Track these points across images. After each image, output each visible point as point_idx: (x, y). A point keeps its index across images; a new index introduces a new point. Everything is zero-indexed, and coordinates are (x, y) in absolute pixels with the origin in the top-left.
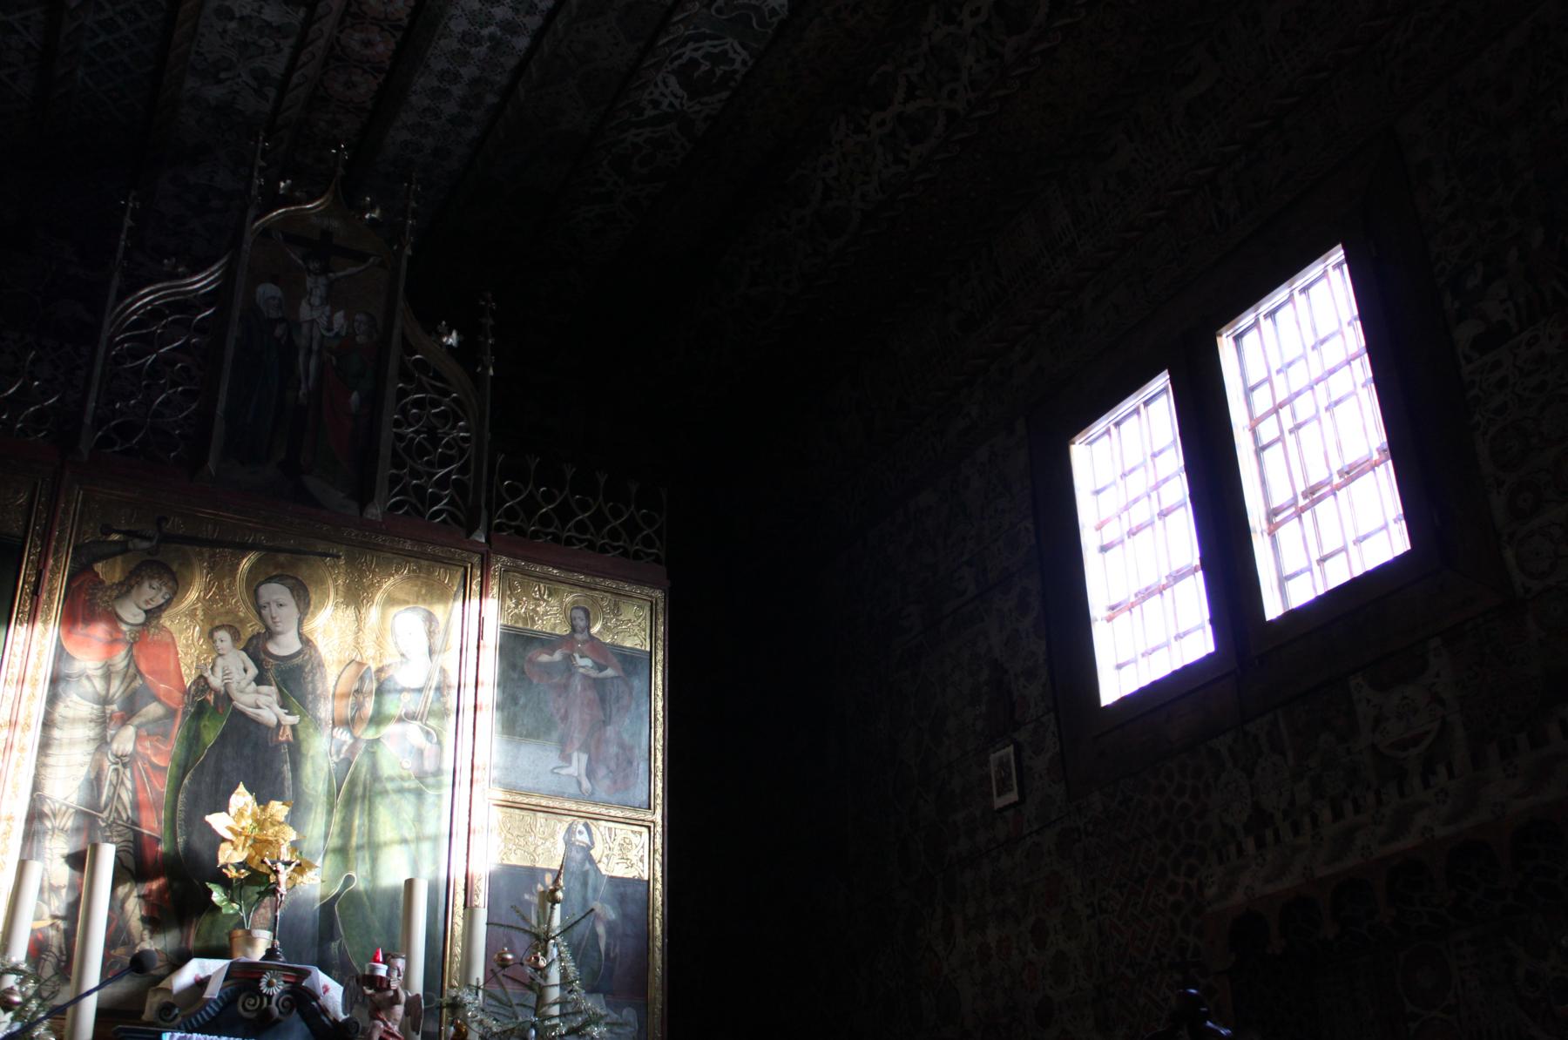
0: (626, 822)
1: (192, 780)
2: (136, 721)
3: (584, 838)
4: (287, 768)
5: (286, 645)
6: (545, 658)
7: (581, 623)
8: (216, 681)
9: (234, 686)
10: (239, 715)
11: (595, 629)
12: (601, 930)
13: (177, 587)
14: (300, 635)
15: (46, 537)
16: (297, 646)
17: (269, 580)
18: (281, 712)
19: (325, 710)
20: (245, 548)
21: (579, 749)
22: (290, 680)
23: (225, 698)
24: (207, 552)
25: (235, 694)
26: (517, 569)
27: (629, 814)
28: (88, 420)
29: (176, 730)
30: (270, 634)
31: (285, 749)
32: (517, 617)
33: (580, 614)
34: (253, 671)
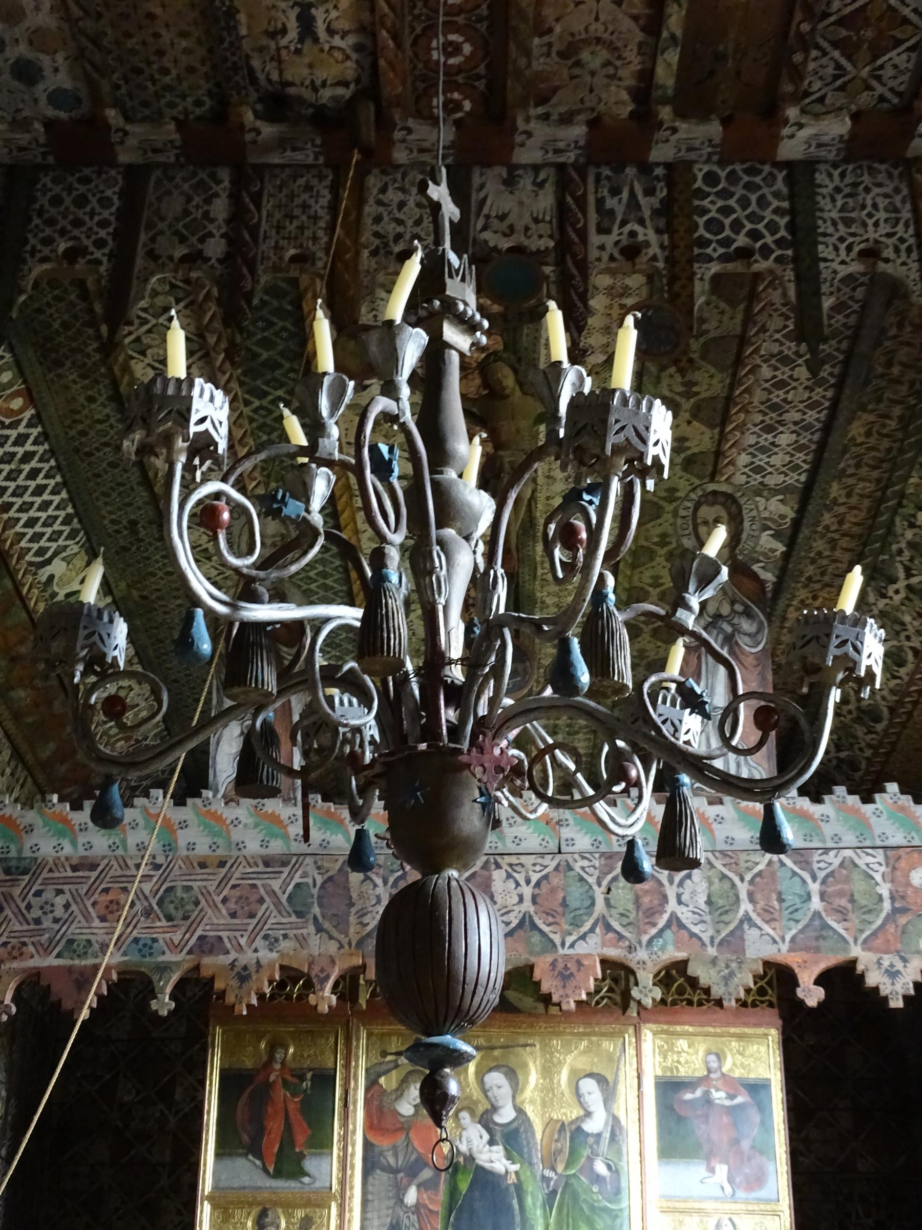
0: (763, 1213)
1: (456, 1219)
2: (416, 1181)
4: (515, 1202)
5: (506, 1115)
6: (688, 1096)
7: (714, 1065)
8: (463, 1148)
9: (475, 1149)
10: (480, 1169)
11: (724, 1070)
14: (515, 1106)
15: (347, 1066)
17: (490, 1070)
18: (507, 1163)
19: (537, 1157)
21: (721, 1162)
22: (512, 1138)
23: (470, 1158)
25: (476, 1155)
26: (663, 1032)
27: (762, 1207)
29: (443, 1187)
30: (495, 1109)
31: (512, 1189)
32: (665, 1069)
33: (713, 1058)
34: (486, 1137)
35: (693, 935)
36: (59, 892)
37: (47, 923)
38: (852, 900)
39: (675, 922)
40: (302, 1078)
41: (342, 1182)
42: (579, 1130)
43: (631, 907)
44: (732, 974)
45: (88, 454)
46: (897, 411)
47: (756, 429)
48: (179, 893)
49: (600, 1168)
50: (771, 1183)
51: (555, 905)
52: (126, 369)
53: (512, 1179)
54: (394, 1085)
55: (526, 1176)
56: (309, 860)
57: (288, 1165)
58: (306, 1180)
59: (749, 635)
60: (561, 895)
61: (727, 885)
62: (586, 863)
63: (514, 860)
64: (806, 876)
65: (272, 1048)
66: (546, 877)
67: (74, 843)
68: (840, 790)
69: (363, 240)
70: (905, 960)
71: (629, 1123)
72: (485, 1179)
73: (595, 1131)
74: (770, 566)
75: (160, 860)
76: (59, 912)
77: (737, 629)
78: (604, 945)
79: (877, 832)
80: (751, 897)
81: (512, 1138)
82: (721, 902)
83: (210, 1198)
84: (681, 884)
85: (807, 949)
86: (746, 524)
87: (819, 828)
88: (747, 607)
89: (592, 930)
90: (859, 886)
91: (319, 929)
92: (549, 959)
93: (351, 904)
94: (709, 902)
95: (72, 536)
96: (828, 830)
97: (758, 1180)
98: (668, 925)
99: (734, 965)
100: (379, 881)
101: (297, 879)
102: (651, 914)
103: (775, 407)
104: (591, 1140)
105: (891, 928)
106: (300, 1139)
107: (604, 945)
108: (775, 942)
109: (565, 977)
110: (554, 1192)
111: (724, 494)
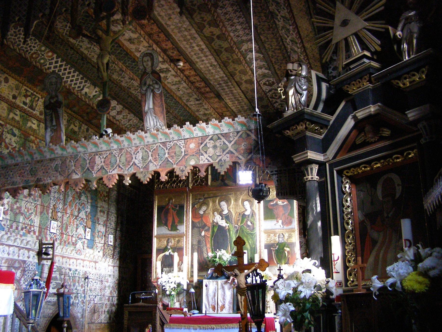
3: (282, 236)
5: (226, 212)
6: (272, 203)
8: (215, 221)
10: (219, 225)
12: (286, 252)
13: (208, 205)
15: (187, 203)
16: (227, 212)
20: (217, 196)
24: (211, 199)
25: (218, 222)
28: (190, 182)
30: (223, 211)
31: (227, 230)
34: (221, 218)
35: (138, 166)
36: (11, 171)
37: (9, 179)
38: (175, 154)
39: (134, 164)
40: (176, 207)
41: (186, 231)
42: (244, 214)
43: (125, 161)
44: (146, 175)
45: (76, 62)
46: (263, 15)
47: (229, 26)
48: (34, 169)
49: (249, 223)
50: (293, 224)
51: (108, 162)
52: (69, 41)
53: (227, 228)
54: (199, 207)
55: (231, 226)
56: (59, 158)
57: (174, 228)
58: (178, 231)
59: (157, 89)
60: (110, 160)
61: (147, 153)
62: (116, 152)
63: (100, 153)
64: (165, 149)
65: (169, 200)
66: (107, 156)
67: (15, 160)
68: (175, 126)
69: (79, 2)
70: (186, 167)
71: (256, 211)
72: (221, 228)
73: (248, 214)
74: (262, 60)
75: (30, 162)
76: (11, 176)
77: (154, 88)
78: (118, 171)
79: (183, 135)
80: (152, 156)
81: (227, 218)
82: (145, 158)
83: (156, 237)
84: (136, 154)
85: (163, 167)
86: (155, 60)
87: (169, 136)
88: (156, 81)
89: (116, 168)
90: (177, 149)
91: (60, 174)
92: (106, 176)
93: (67, 167)
94: (142, 158)
95: (86, 82)
96: (171, 136)
97: (290, 223)
98: (132, 165)
99: (146, 173)
100: (72, 161)
101: (56, 163)
102: (129, 162)
103: (229, 20)
104: (247, 216)
105: (183, 159)
106: (176, 221)
107: (118, 171)
108: (156, 166)
109: (109, 180)
110: (238, 230)
111: (149, 53)
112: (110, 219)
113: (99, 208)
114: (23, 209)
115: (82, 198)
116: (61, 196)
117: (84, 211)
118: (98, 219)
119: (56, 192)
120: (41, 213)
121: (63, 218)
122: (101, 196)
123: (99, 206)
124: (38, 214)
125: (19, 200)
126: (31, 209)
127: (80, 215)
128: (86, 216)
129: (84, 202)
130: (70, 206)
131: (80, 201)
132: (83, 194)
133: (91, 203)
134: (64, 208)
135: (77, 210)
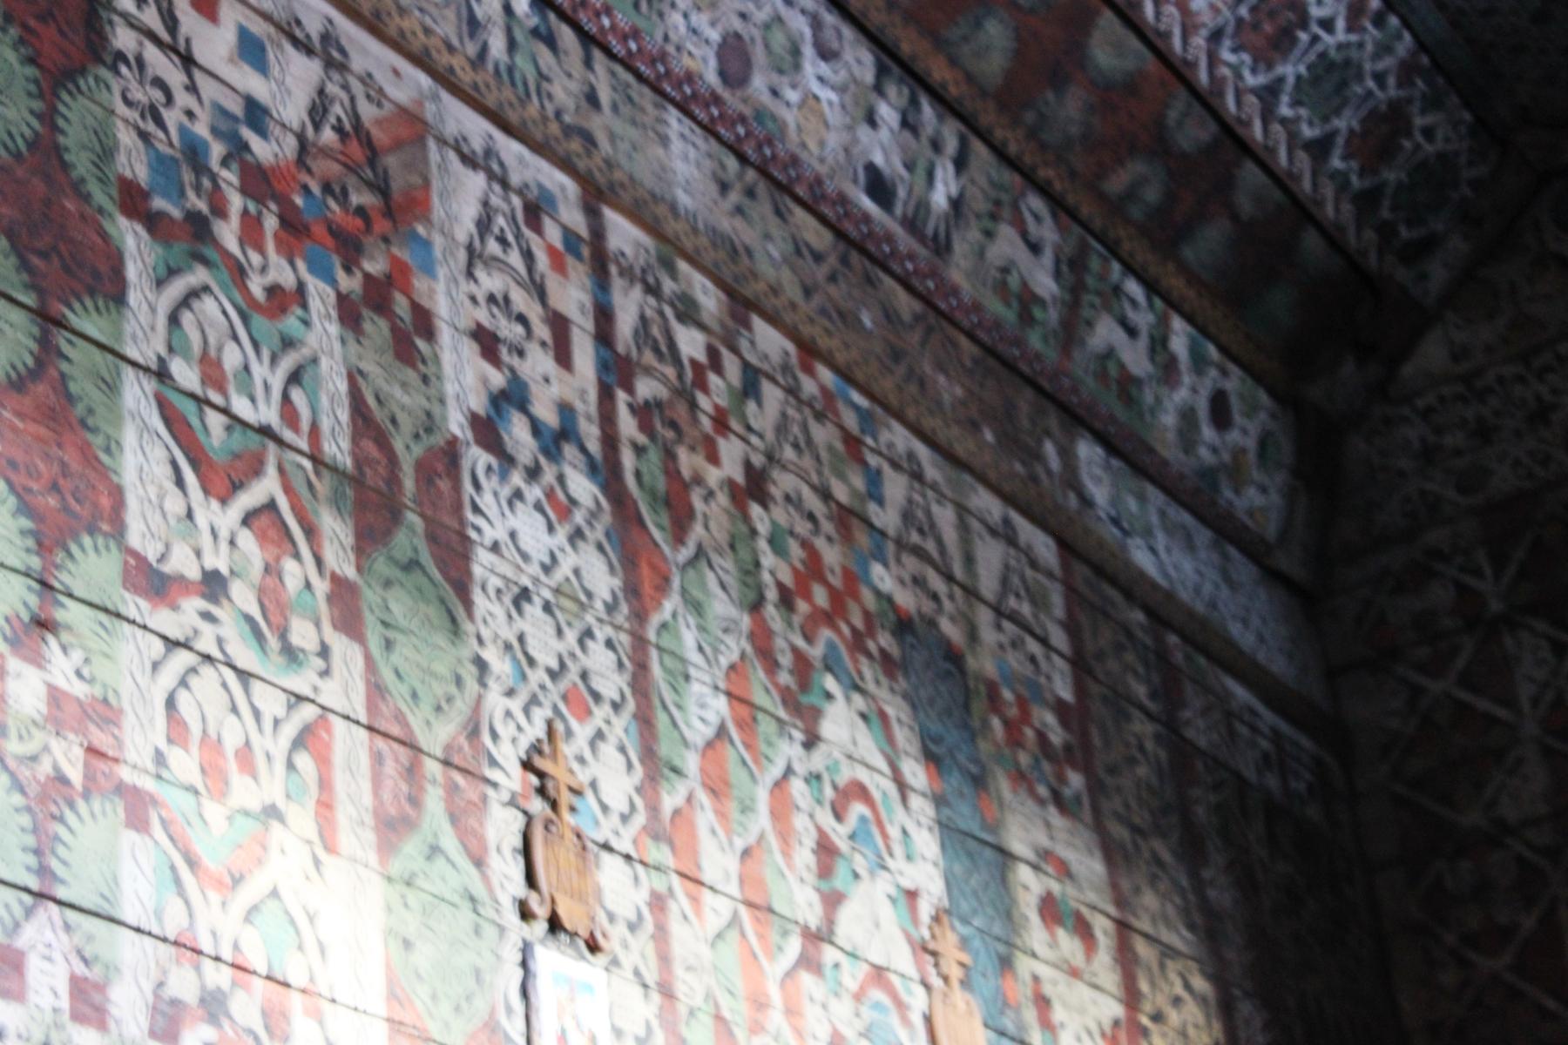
112: (1157, 1017)
113: (1024, 873)
114: (141, 736)
115: (827, 728)
116: (600, 659)
117: (882, 886)
118: (1043, 1003)
119: (524, 595)
120: (392, 827)
121: (661, 935)
122: (1014, 739)
123: (1018, 847)
124: (356, 837)
125: (71, 613)
126: (245, 755)
127: (849, 923)
128: (926, 951)
129: (863, 775)
130: (714, 792)
131: (817, 761)
132: (830, 683)
133: (939, 801)
134: (654, 809)
135: (805, 856)
